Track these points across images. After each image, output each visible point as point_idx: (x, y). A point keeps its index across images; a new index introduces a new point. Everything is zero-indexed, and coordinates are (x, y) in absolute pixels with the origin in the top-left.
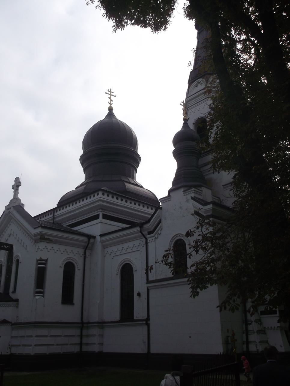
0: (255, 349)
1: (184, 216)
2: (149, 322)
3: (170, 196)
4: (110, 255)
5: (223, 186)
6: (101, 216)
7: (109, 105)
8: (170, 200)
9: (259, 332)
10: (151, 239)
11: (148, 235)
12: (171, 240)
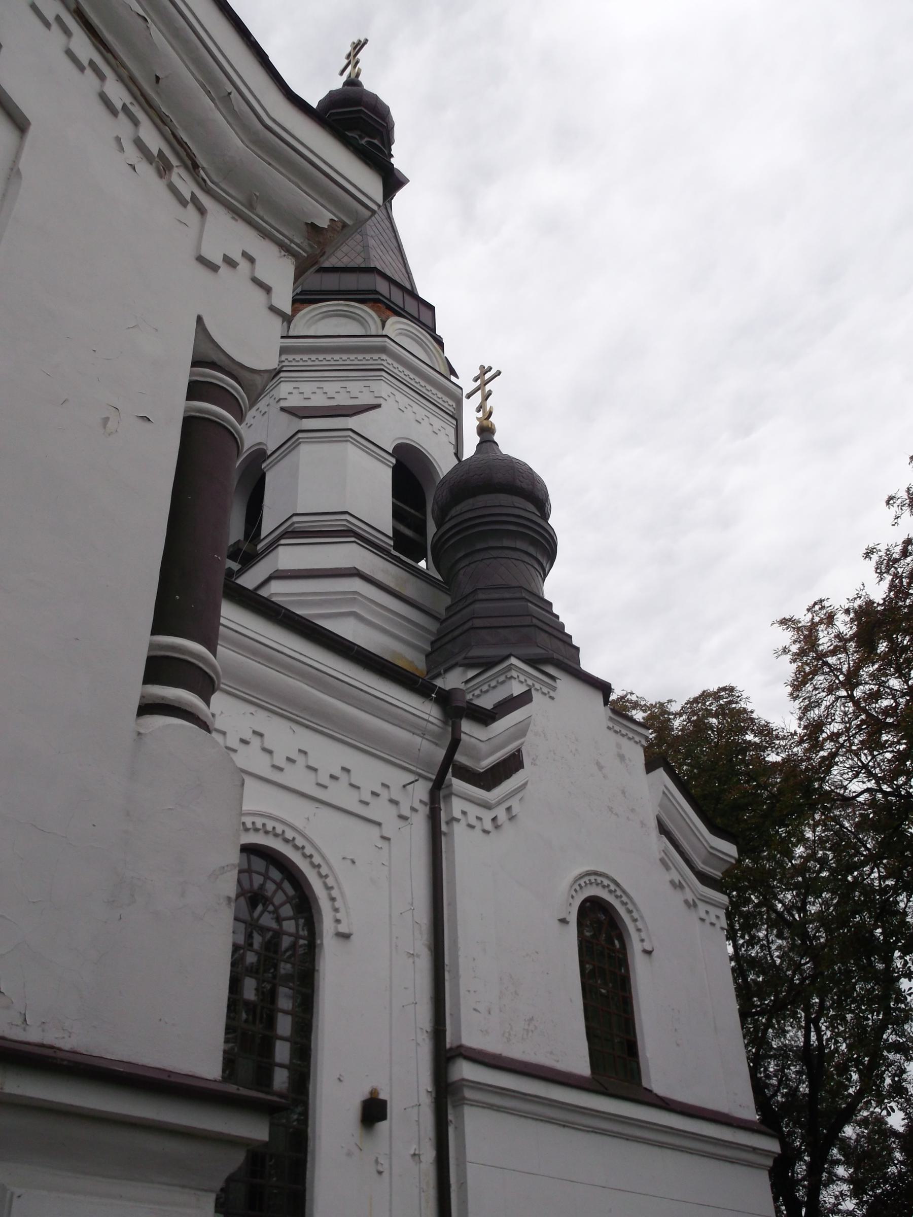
1: (616, 815)
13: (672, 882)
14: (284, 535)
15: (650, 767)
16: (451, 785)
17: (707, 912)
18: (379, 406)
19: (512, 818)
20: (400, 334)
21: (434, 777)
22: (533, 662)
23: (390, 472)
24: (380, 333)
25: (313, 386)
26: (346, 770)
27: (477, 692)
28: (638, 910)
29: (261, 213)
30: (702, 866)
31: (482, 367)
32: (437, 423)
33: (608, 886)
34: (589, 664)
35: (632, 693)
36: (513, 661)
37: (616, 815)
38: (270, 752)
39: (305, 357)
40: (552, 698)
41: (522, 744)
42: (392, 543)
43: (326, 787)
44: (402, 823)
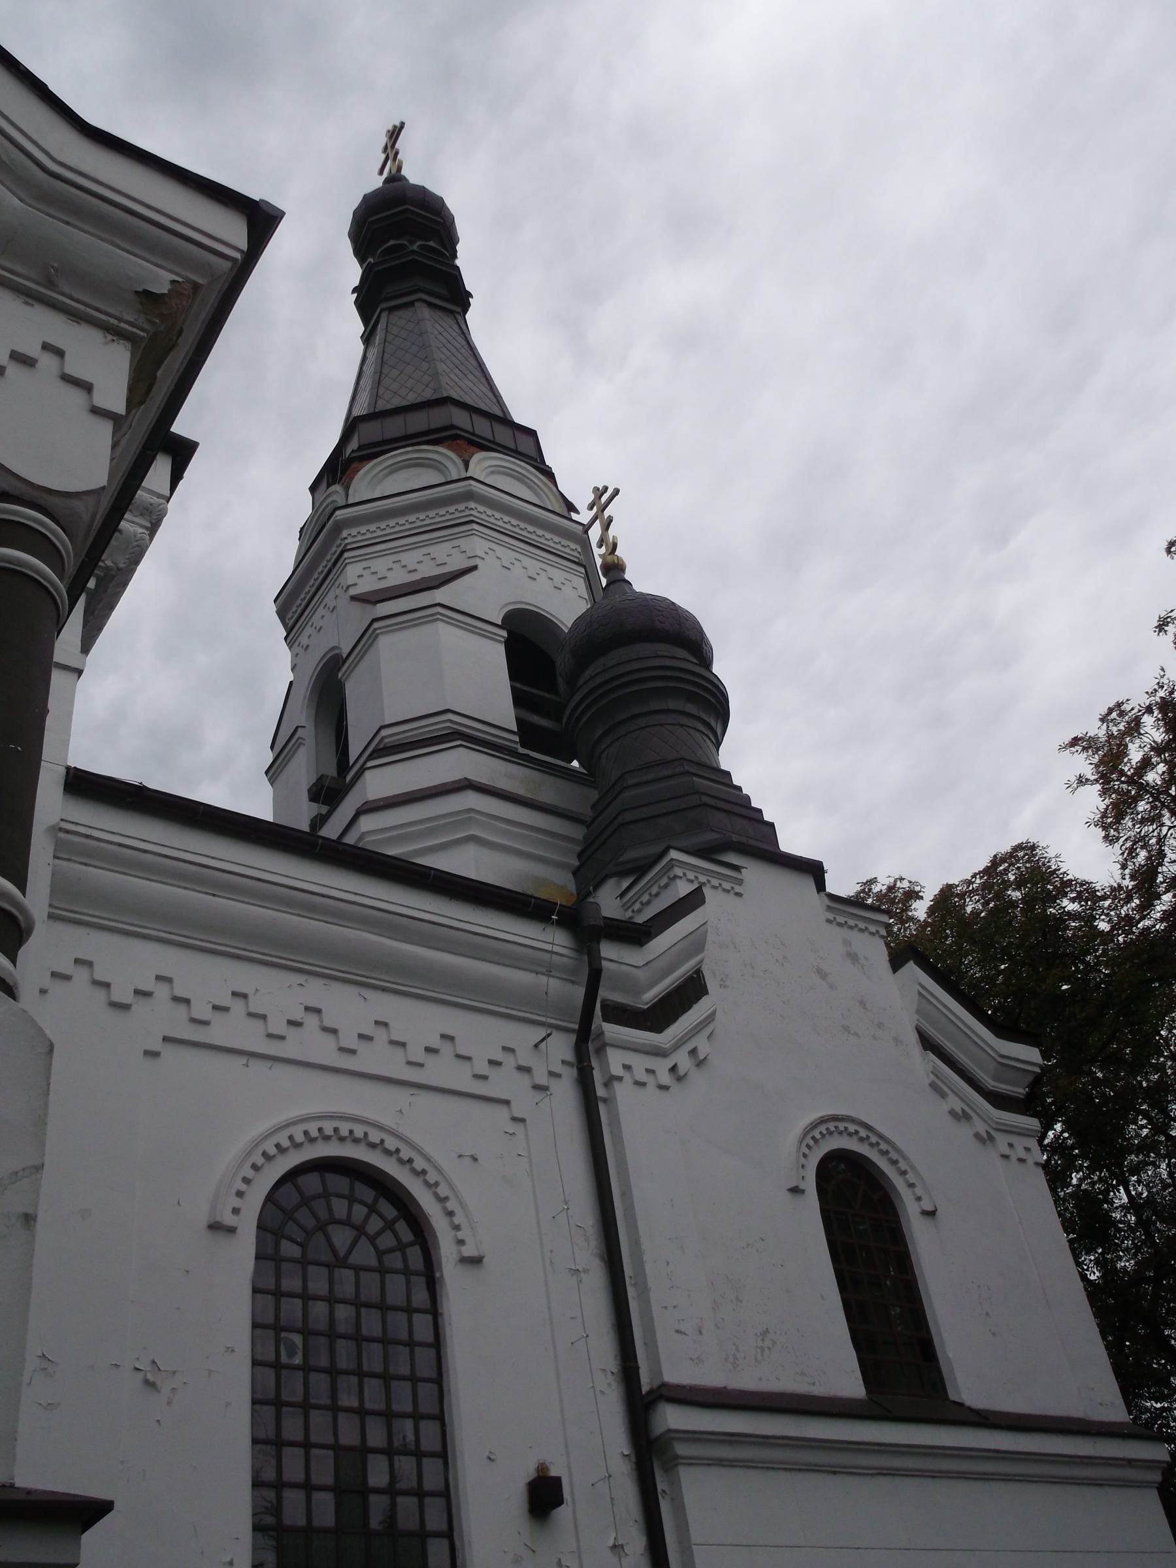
1: (856, 1034)
8: (738, 889)
13: (952, 1113)
14: (371, 757)
15: (896, 962)
16: (601, 1034)
17: (1011, 1145)
18: (475, 568)
19: (701, 1064)
20: (492, 472)
21: (576, 1027)
22: (706, 852)
23: (501, 649)
24: (464, 475)
25: (388, 561)
26: (447, 1038)
27: (637, 906)
28: (905, 1158)
29: (67, 290)
30: (993, 1083)
31: (596, 489)
32: (559, 575)
33: (857, 1132)
34: (790, 842)
35: (902, 879)
36: (674, 854)
37: (856, 1034)
38: (334, 1032)
39: (372, 527)
40: (739, 895)
41: (702, 961)
42: (517, 739)
43: (421, 1065)
44: (538, 1096)
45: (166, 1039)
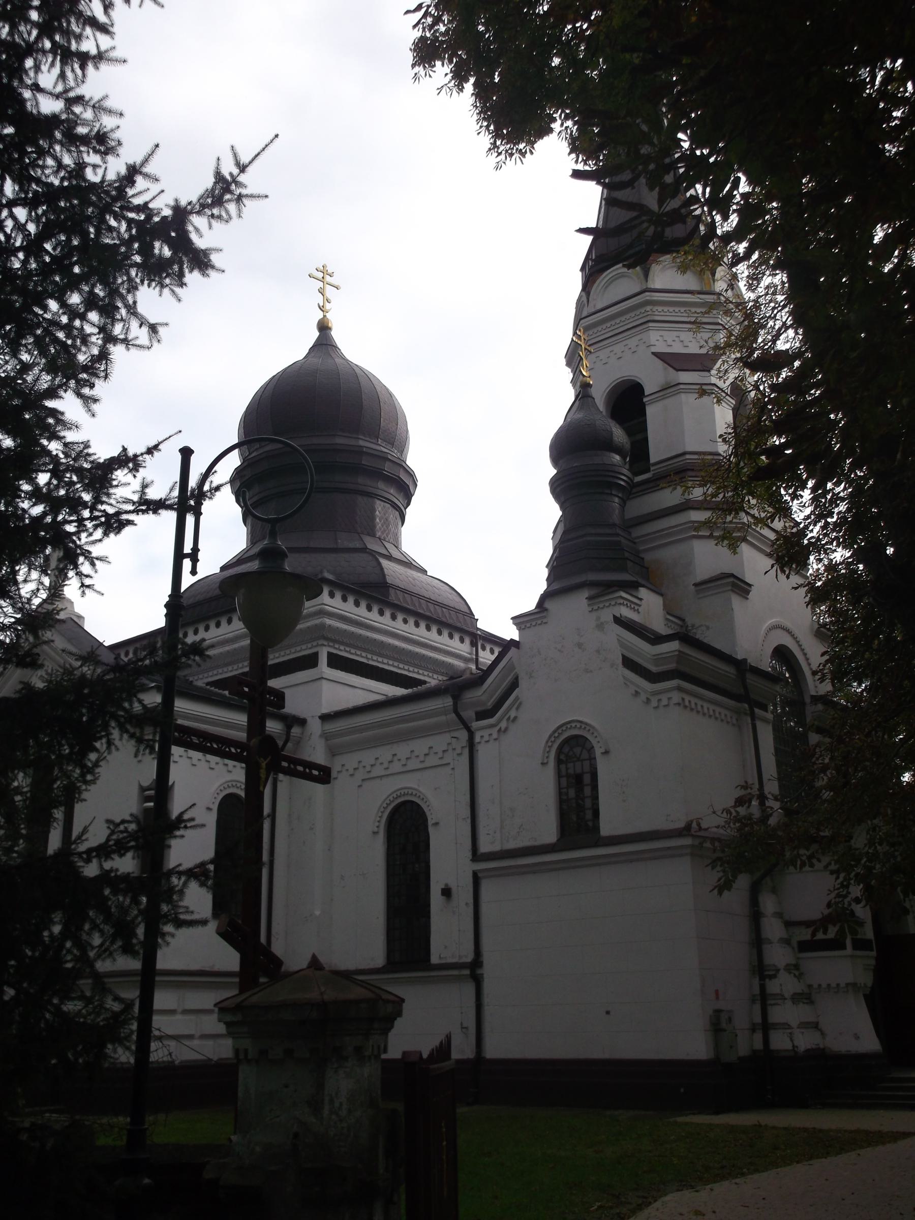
0: (789, 1046)
1: (591, 671)
2: (479, 972)
3: (546, 610)
4: (352, 775)
5: (696, 585)
6: (323, 659)
7: (320, 315)
8: (545, 621)
9: (798, 998)
10: (488, 731)
11: (477, 720)
12: (550, 737)
45: (363, 780)
